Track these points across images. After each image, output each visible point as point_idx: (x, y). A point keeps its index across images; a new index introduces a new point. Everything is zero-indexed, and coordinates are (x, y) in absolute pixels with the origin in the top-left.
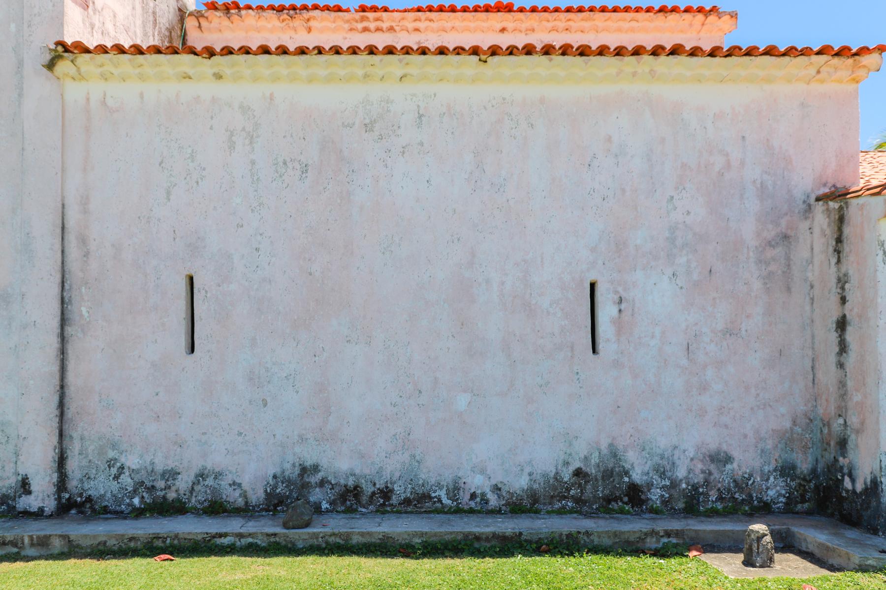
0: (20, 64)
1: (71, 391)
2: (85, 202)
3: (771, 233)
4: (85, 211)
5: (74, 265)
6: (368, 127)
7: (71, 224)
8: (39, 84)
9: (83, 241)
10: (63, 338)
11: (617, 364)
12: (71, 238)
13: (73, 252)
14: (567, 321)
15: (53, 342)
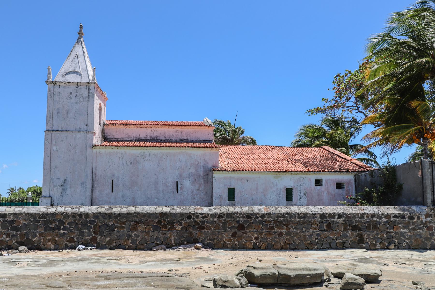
0: (86, 146)
1: (93, 198)
2: (96, 168)
3: (205, 174)
4: (96, 170)
5: (94, 178)
6: (141, 157)
7: (94, 171)
8: (89, 150)
9: (95, 174)
10: (92, 190)
11: (181, 195)
12: (94, 174)
13: (94, 176)
14: (172, 187)
15: (91, 190)
